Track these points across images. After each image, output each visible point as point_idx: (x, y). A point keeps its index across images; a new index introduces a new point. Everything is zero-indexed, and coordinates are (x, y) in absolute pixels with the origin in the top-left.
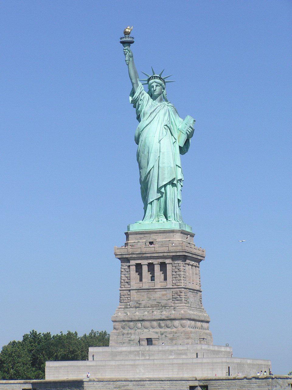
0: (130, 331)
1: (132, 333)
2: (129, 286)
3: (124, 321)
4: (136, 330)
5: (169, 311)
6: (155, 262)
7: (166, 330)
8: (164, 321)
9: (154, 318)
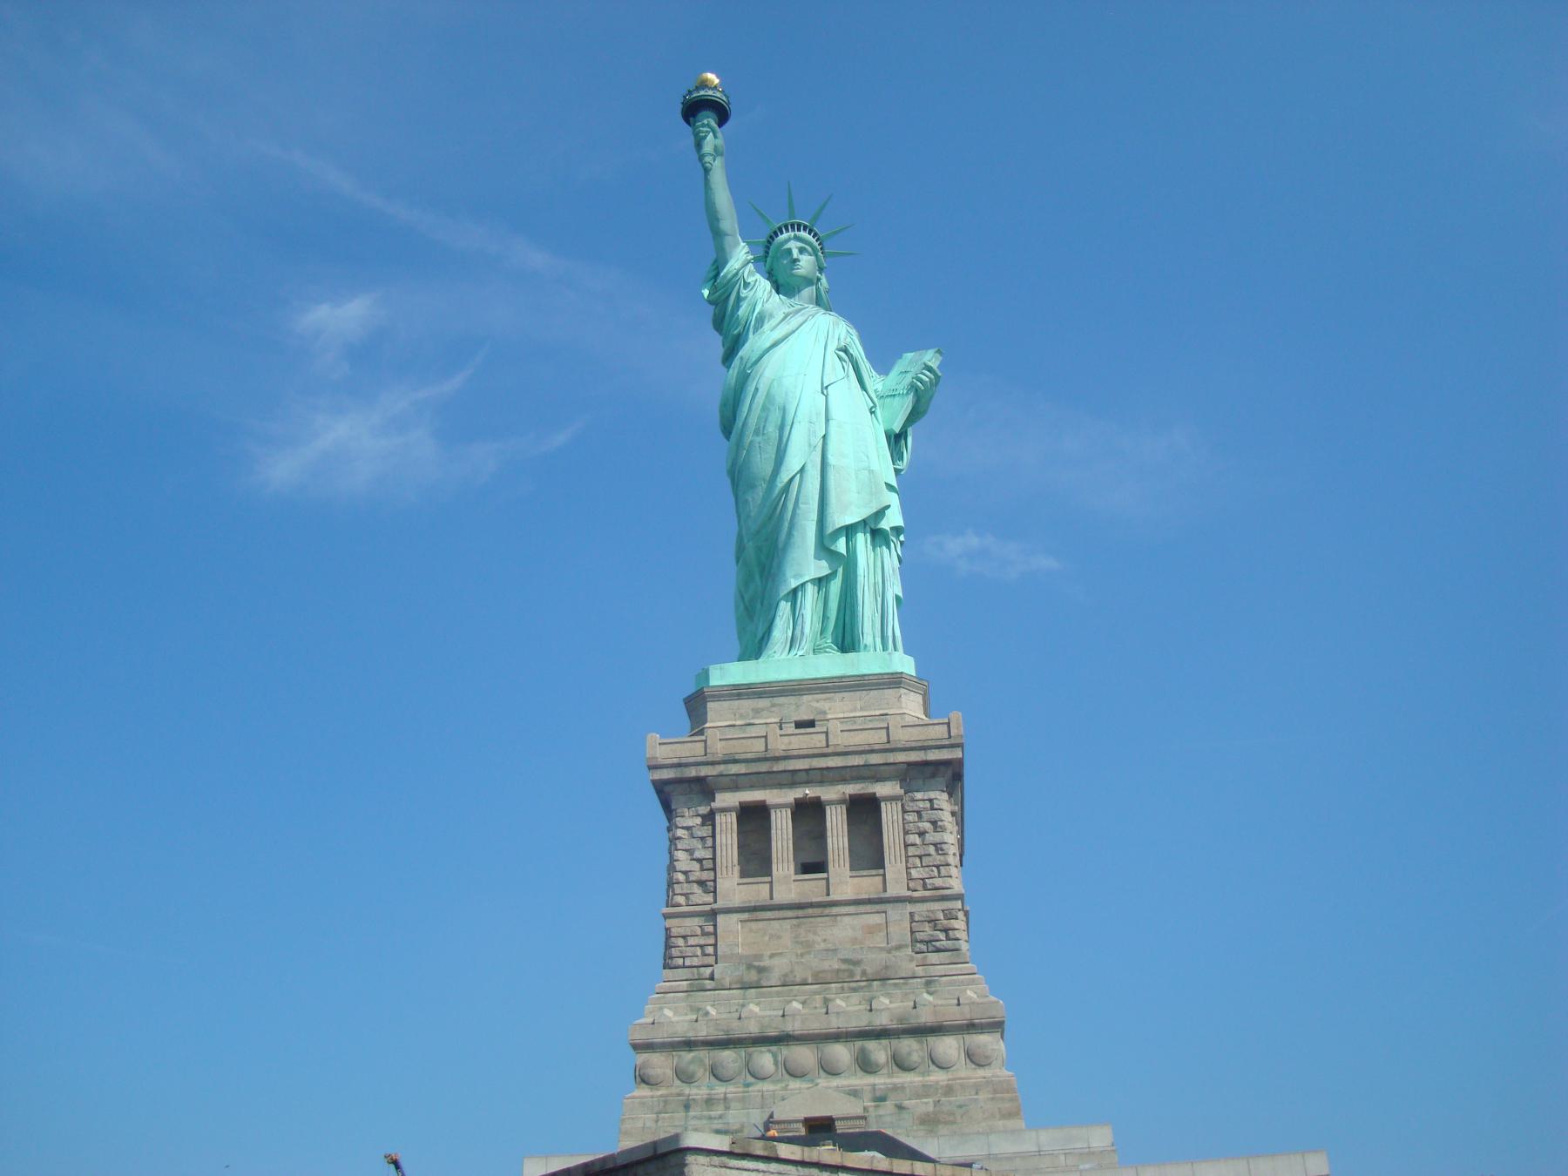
0: (720, 1089)
1: (728, 1095)
2: (709, 898)
3: (689, 1045)
4: (748, 1085)
5: (906, 994)
6: (828, 793)
7: (895, 1080)
8: (885, 1042)
9: (836, 1024)
